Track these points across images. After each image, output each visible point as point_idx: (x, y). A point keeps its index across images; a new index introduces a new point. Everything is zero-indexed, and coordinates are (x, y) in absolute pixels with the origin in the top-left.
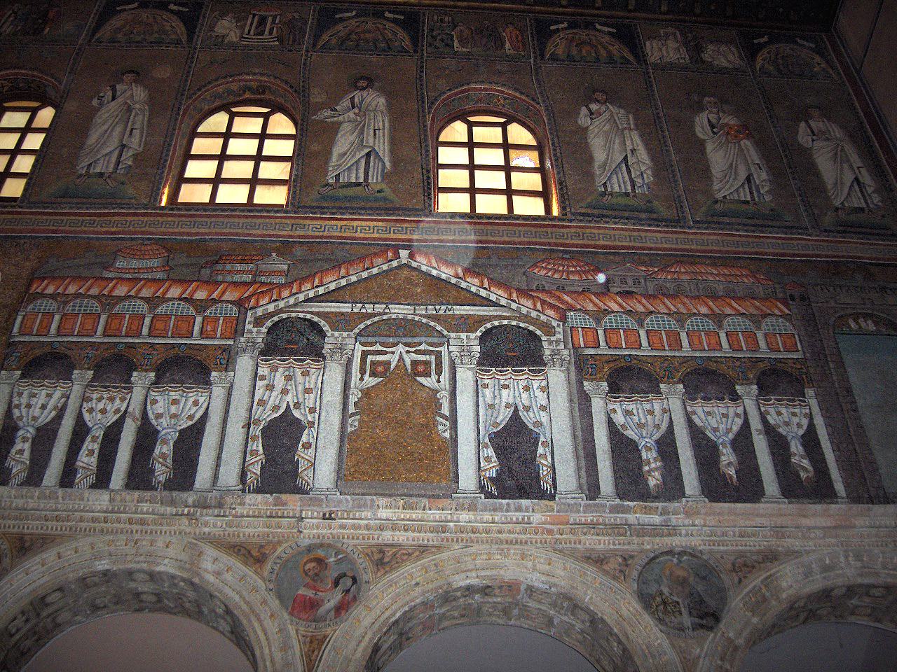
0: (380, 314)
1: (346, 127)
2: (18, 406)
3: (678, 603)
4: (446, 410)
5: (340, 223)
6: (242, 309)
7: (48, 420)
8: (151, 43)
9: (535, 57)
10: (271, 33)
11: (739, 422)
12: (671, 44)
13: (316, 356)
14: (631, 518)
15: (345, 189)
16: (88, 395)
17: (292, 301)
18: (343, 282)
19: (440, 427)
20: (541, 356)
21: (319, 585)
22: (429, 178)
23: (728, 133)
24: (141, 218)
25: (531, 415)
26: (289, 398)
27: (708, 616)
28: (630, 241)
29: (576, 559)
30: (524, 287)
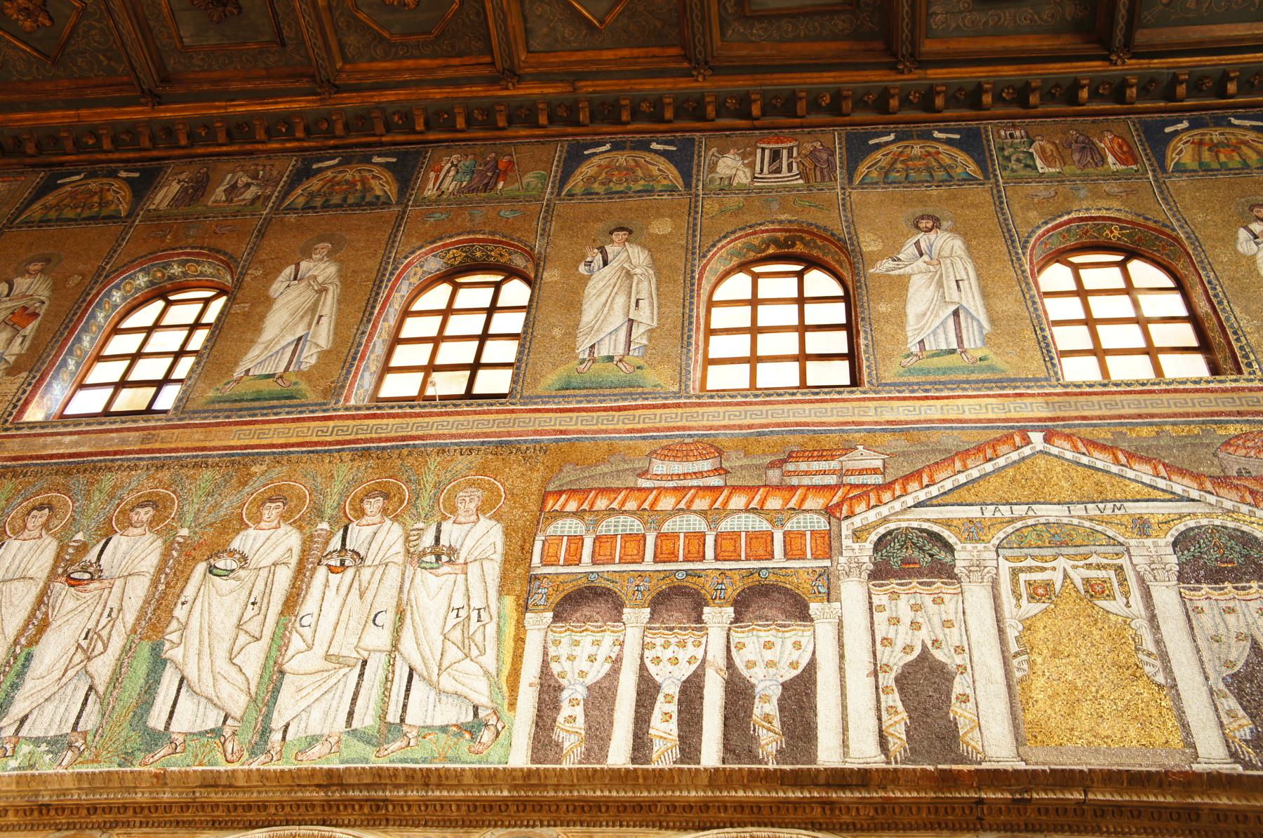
0: (1021, 518)
4: (1149, 645)
6: (833, 520)
9: (1154, 171)
15: (936, 359)
16: (647, 640)
17: (897, 505)
18: (962, 478)
19: (1147, 669)
22: (1045, 337)
30: (1217, 471)
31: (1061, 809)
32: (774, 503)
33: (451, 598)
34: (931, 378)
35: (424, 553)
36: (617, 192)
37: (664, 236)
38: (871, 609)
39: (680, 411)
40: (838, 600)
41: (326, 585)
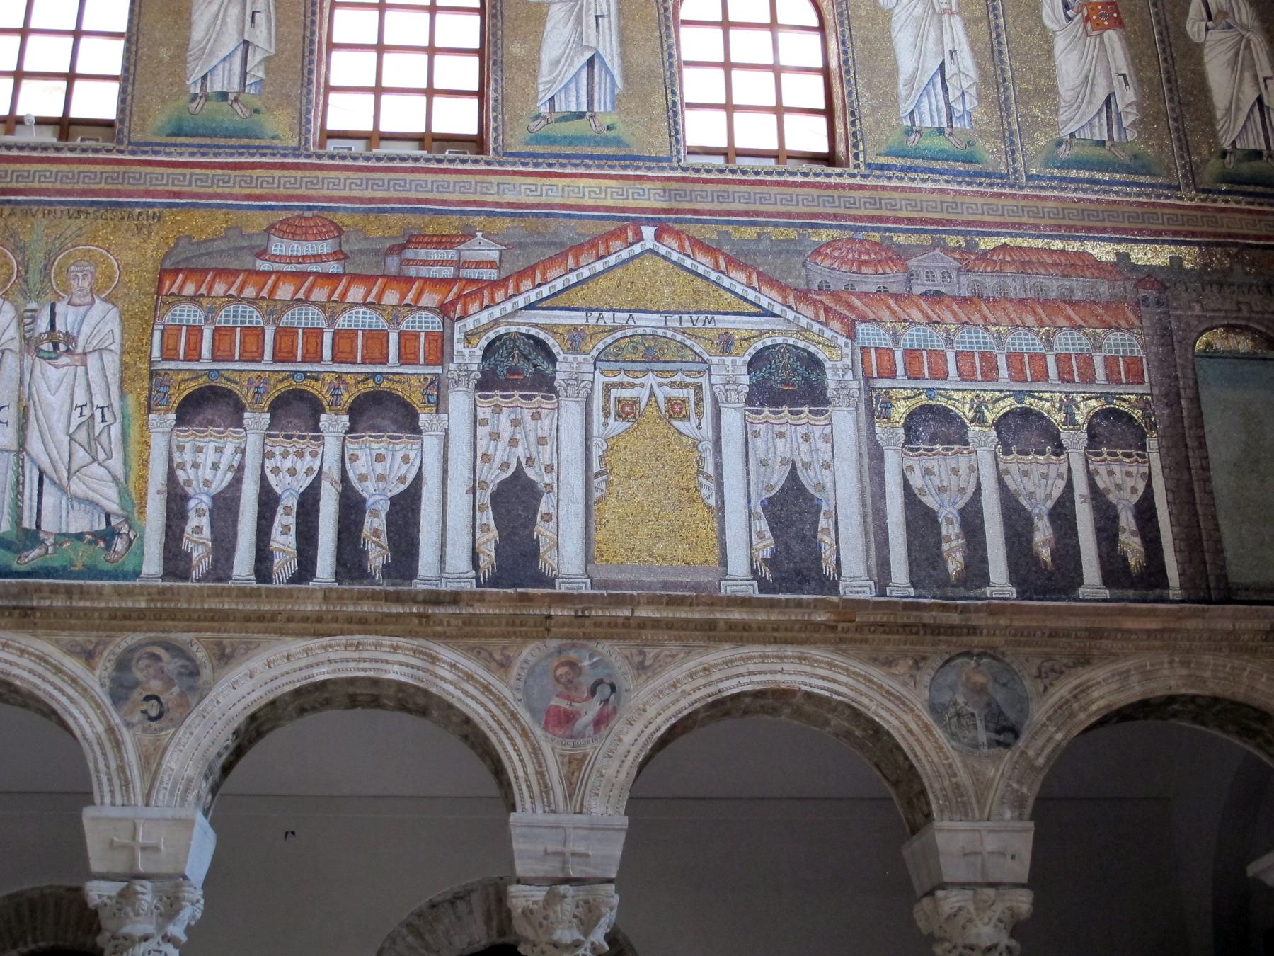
0: (622, 327)
2: (182, 465)
3: (973, 715)
4: (710, 469)
6: (448, 321)
7: (224, 484)
11: (1061, 485)
13: (548, 391)
14: (927, 617)
16: (268, 448)
17: (509, 307)
18: (573, 278)
19: (704, 491)
21: (573, 694)
22: (674, 103)
23: (1087, 19)
24: (293, 173)
25: (812, 474)
26: (520, 451)
27: (1006, 731)
28: (942, 211)
29: (861, 661)
30: (801, 284)
31: (612, 624)
32: (391, 298)
33: (72, 394)
34: (556, 149)
35: (40, 341)
38: (475, 422)
39: (299, 174)
40: (447, 412)
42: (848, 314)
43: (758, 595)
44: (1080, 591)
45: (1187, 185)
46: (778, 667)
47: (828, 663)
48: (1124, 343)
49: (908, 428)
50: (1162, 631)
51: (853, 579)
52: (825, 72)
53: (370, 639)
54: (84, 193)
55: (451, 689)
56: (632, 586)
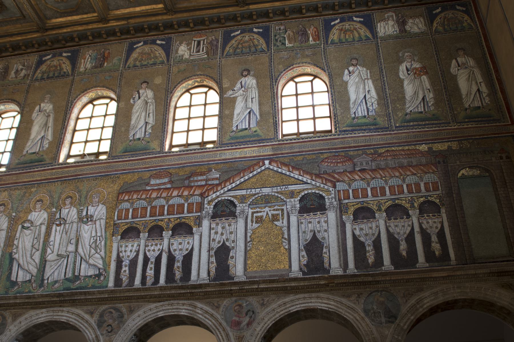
0: (258, 194)
1: (239, 99)
2: (121, 252)
3: (380, 312)
5: (239, 150)
8: (152, 64)
9: (324, 44)
10: (203, 51)
11: (409, 229)
12: (391, 23)
14: (360, 279)
17: (222, 191)
18: (242, 180)
19: (284, 244)
20: (324, 205)
22: (276, 121)
23: (415, 73)
24: (158, 159)
25: (321, 234)
26: (224, 237)
30: (317, 172)
32: (186, 193)
34: (238, 141)
35: (83, 218)
36: (144, 65)
37: (159, 84)
39: (160, 159)
40: (202, 227)
41: (56, 231)
42: (332, 179)
43: (302, 276)
44: (417, 265)
45: (453, 121)
46: (310, 301)
47: (327, 298)
48: (431, 177)
49: (354, 215)
50: (448, 276)
51: (335, 268)
52: (329, 105)
53: (176, 302)
54: (98, 173)
55: (201, 316)
56: (259, 277)
